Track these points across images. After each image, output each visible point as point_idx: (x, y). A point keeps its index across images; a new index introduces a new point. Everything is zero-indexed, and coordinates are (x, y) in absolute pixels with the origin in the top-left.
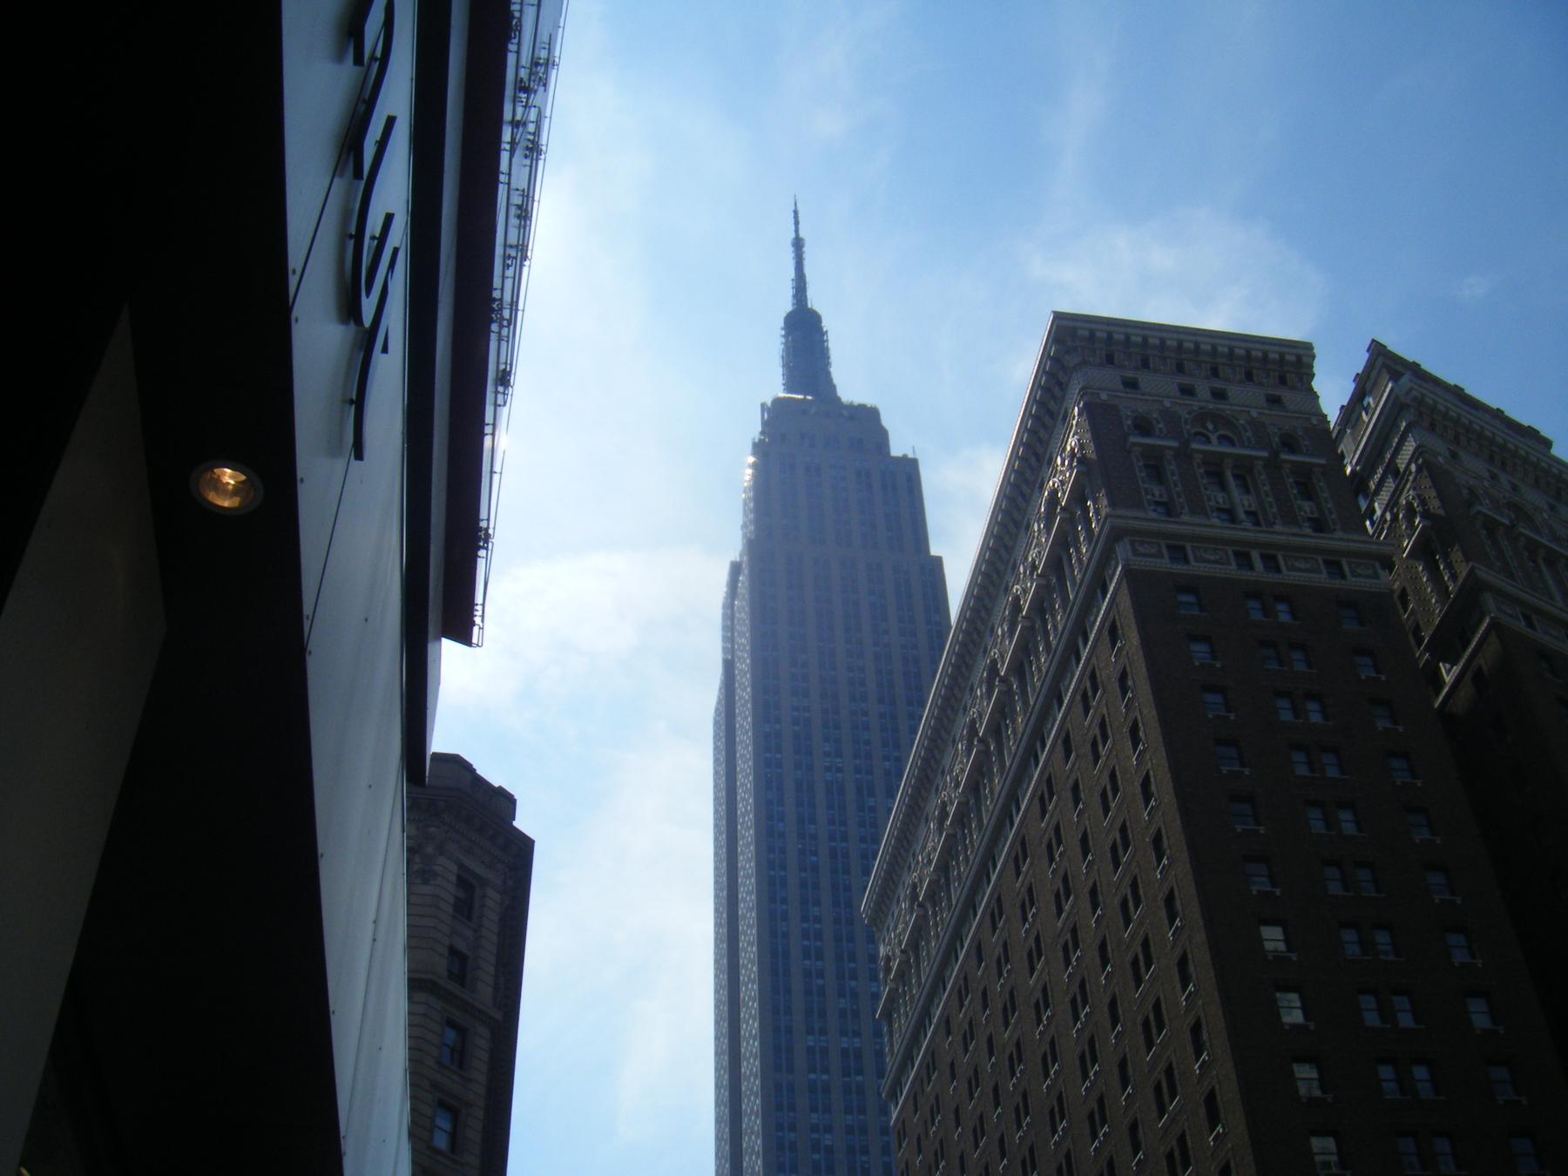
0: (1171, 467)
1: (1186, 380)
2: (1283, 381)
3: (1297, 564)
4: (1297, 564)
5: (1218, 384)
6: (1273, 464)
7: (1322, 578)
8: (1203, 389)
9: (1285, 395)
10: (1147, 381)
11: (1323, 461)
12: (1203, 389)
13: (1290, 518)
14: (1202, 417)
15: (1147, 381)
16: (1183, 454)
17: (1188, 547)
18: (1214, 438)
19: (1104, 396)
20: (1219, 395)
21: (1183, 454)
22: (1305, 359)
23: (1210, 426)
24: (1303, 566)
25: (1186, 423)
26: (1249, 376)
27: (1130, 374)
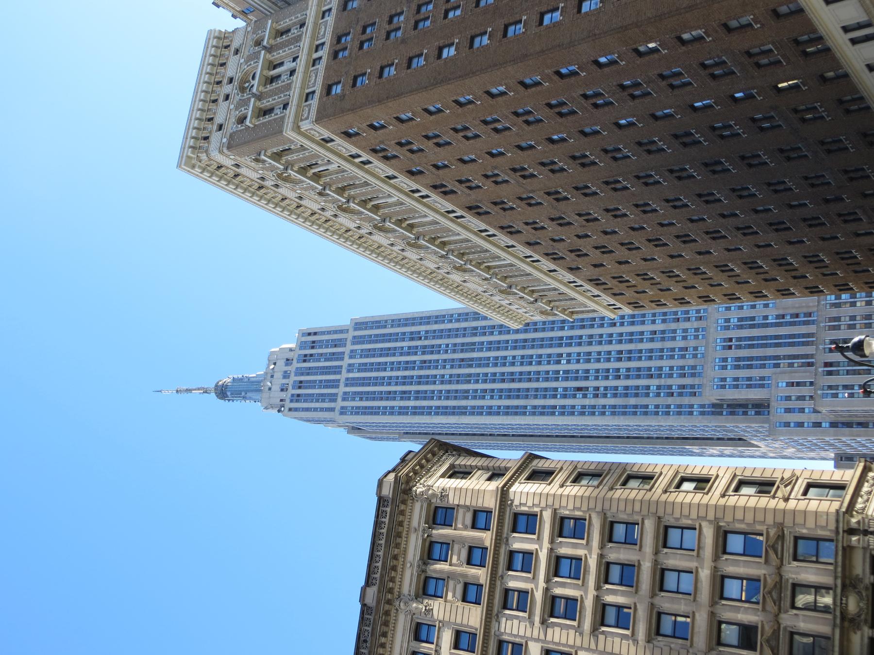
0: (266, 104)
1: (221, 98)
2: (227, 47)
3: (322, 33)
4: (322, 33)
5: (225, 81)
6: (269, 49)
7: (330, 19)
8: (227, 89)
9: (235, 45)
11: (270, 21)
12: (227, 89)
13: (298, 39)
16: (259, 97)
17: (307, 91)
18: (253, 82)
19: (225, 140)
20: (231, 80)
21: (259, 97)
22: (216, 34)
23: (247, 85)
24: (323, 30)
25: (243, 96)
26: (223, 65)
27: (215, 127)
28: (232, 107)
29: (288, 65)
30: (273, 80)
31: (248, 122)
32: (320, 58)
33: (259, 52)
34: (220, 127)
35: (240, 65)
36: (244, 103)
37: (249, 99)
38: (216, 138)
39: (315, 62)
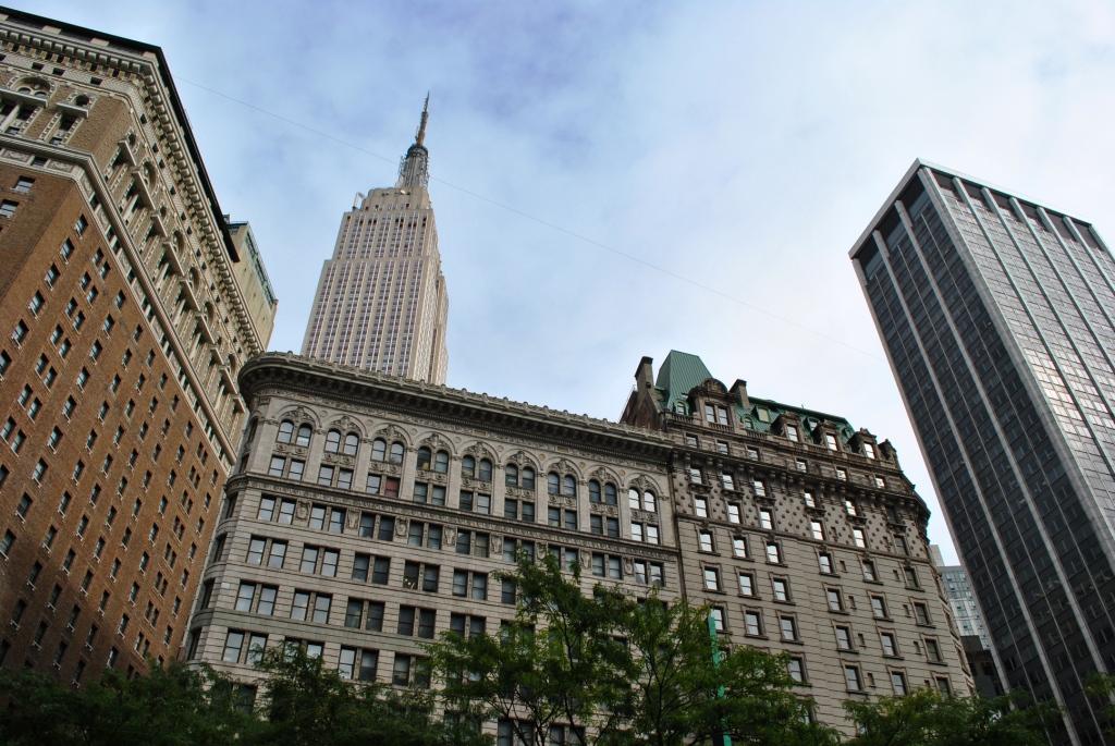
8: (159, 157)
10: (148, 127)
12: (159, 157)
14: (148, 165)
15: (148, 127)
19: (132, 111)
20: (162, 165)
28: (146, 145)
29: (128, 215)
30: (131, 194)
31: (127, 143)
32: (110, 240)
33: (157, 204)
34: (143, 120)
35: (165, 184)
36: (140, 155)
37: (138, 161)
38: (138, 107)
39: (112, 233)
